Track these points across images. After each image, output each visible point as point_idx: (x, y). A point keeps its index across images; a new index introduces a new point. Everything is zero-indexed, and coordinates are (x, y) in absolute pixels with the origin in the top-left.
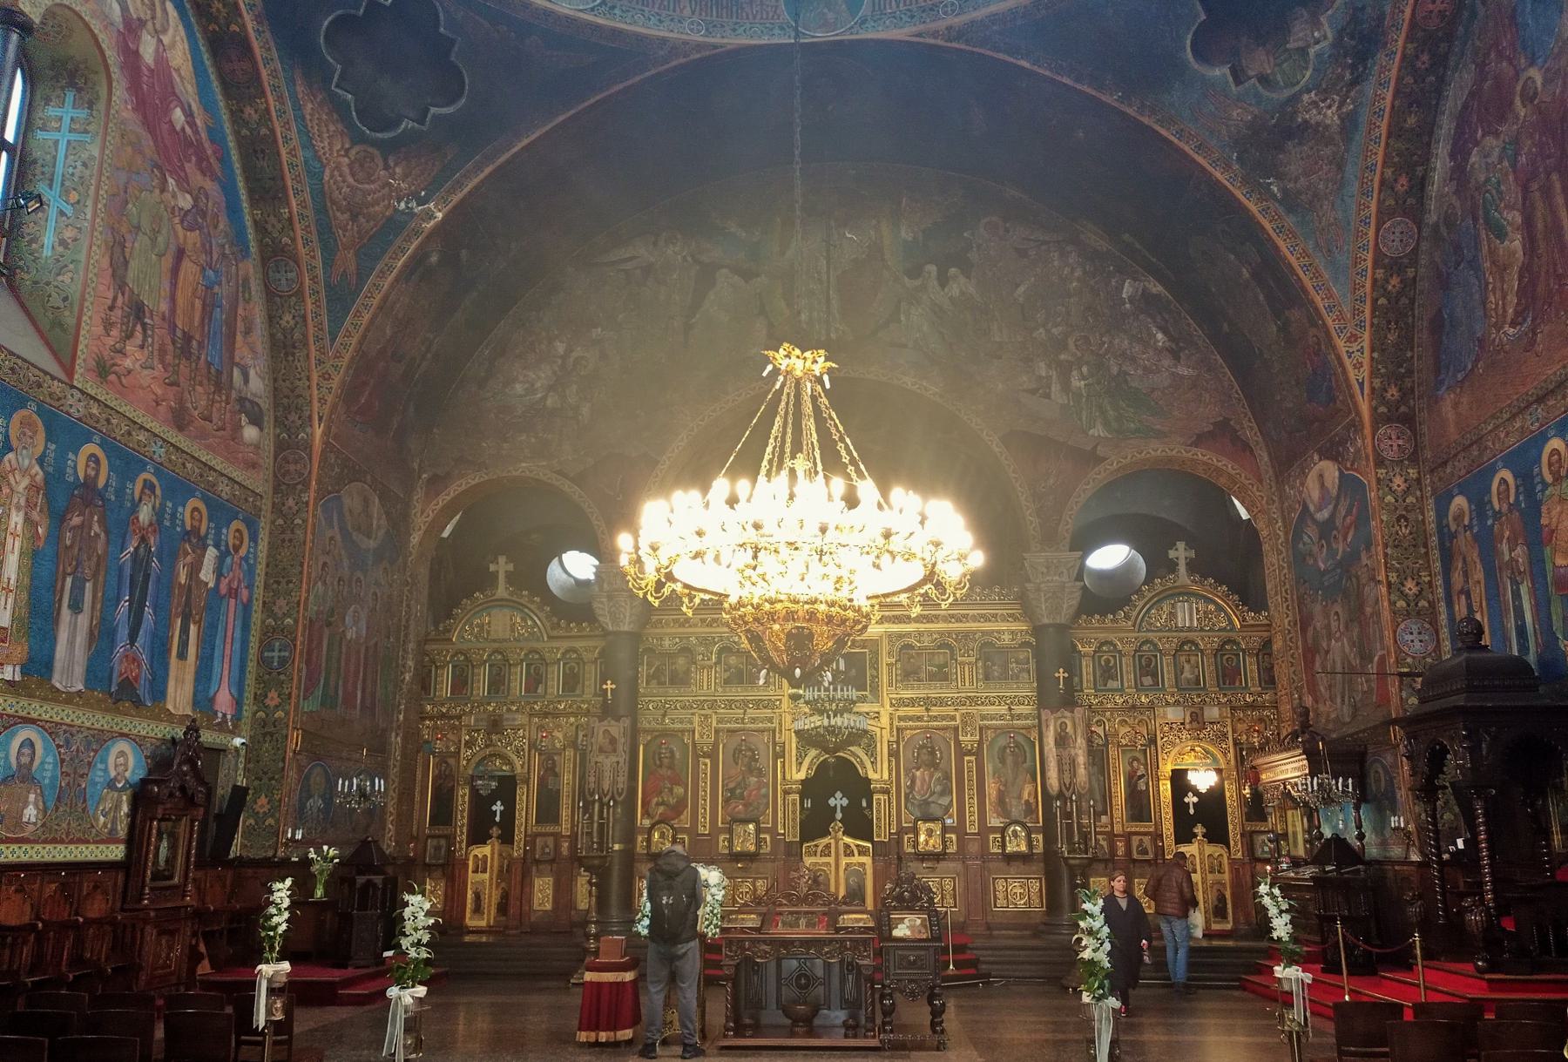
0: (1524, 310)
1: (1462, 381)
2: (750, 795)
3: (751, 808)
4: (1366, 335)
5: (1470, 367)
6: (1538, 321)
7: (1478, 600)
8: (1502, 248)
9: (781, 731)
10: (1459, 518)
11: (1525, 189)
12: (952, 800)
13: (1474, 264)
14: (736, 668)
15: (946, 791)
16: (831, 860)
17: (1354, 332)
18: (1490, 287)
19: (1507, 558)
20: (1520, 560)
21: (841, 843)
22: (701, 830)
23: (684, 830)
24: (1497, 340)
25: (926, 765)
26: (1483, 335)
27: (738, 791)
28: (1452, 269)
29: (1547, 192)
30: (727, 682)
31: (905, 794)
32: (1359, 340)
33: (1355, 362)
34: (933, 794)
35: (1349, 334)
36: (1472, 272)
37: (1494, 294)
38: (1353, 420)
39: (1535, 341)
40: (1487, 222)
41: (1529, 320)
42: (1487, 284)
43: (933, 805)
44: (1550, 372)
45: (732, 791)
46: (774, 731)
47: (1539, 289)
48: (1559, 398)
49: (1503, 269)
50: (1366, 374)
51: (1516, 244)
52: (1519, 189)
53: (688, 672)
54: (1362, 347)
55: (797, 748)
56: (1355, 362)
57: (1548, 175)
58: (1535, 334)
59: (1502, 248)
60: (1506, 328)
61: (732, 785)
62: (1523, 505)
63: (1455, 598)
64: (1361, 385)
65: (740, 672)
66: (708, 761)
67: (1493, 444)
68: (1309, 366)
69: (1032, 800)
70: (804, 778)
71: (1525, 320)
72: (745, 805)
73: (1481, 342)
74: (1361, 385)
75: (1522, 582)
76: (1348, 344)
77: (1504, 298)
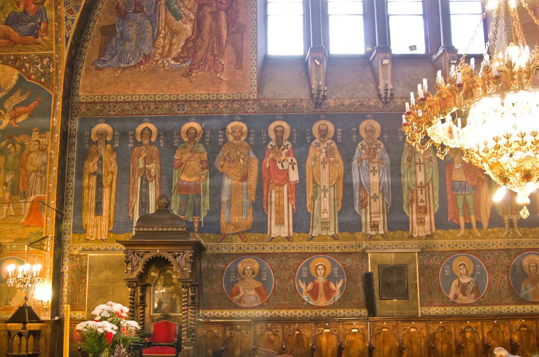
0: (185, 57)
1: (124, 68)
4: (78, 15)
5: (133, 64)
6: (195, 67)
7: (109, 182)
8: (176, 24)
10: (102, 134)
11: (201, 7)
13: (153, 19)
17: (73, 9)
18: (162, 35)
19: (141, 166)
20: (153, 170)
24: (160, 62)
26: (150, 54)
28: (131, 11)
29: (216, 17)
32: (74, 15)
33: (68, 25)
35: (69, 8)
36: (148, 21)
37: (164, 40)
38: (52, 55)
39: (191, 75)
40: (167, 4)
41: (188, 64)
42: (159, 33)
44: (198, 93)
47: (199, 53)
48: (202, 106)
49: (174, 33)
50: (71, 35)
51: (189, 27)
52: (197, 5)
54: (74, 20)
56: (68, 25)
57: (219, 10)
58: (191, 70)
59: (176, 24)
60: (170, 59)
62: (162, 145)
63: (86, 176)
64: (67, 39)
67: (143, 108)
68: (22, 6)
71: (185, 62)
73: (147, 58)
74: (67, 39)
75: (152, 181)
76: (67, 13)
77: (171, 45)
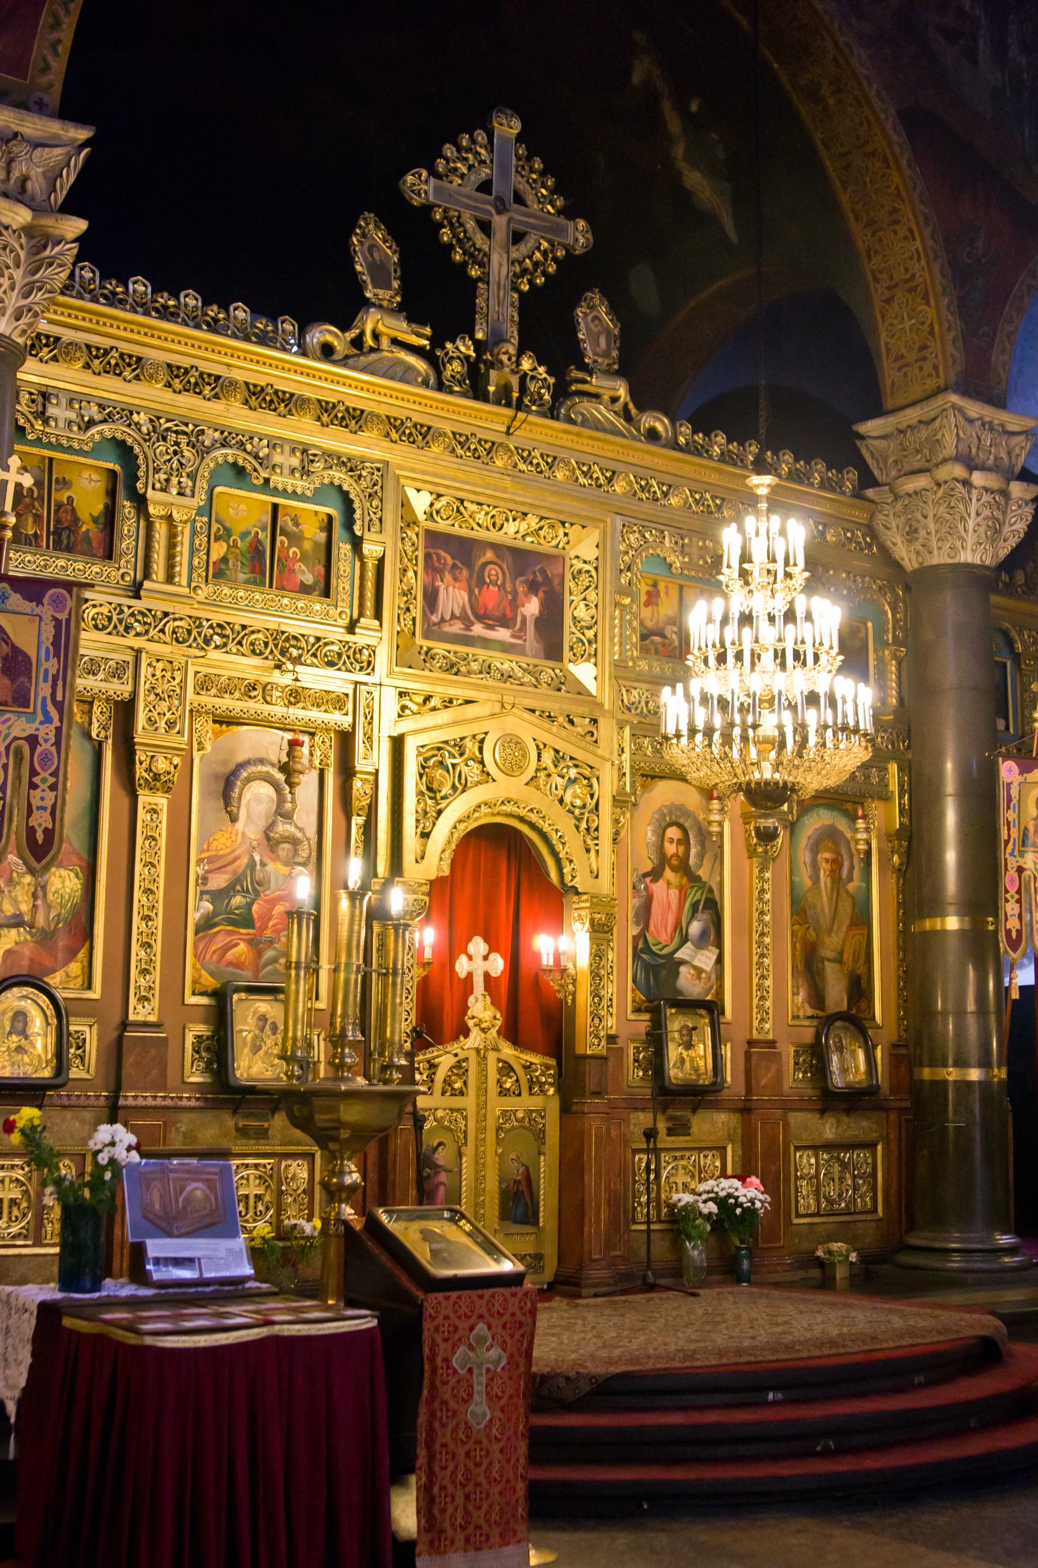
2: (267, 916)
3: (270, 954)
9: (370, 739)
12: (720, 960)
14: (244, 535)
15: (714, 935)
16: (469, 1102)
21: (492, 1056)
22: (138, 1013)
23: (87, 1009)
25: (674, 869)
27: (238, 900)
30: (219, 572)
31: (634, 937)
34: (684, 940)
43: (683, 969)
45: (218, 896)
46: (345, 740)
53: (109, 517)
55: (421, 793)
61: (219, 881)
65: (256, 550)
66: (161, 801)
69: (861, 970)
70: (433, 877)
72: (251, 942)
